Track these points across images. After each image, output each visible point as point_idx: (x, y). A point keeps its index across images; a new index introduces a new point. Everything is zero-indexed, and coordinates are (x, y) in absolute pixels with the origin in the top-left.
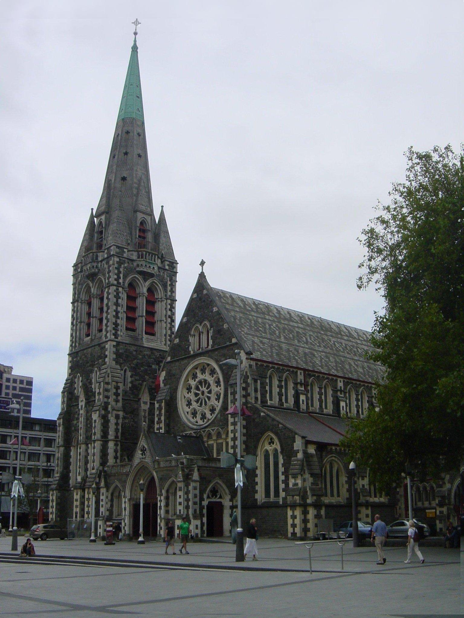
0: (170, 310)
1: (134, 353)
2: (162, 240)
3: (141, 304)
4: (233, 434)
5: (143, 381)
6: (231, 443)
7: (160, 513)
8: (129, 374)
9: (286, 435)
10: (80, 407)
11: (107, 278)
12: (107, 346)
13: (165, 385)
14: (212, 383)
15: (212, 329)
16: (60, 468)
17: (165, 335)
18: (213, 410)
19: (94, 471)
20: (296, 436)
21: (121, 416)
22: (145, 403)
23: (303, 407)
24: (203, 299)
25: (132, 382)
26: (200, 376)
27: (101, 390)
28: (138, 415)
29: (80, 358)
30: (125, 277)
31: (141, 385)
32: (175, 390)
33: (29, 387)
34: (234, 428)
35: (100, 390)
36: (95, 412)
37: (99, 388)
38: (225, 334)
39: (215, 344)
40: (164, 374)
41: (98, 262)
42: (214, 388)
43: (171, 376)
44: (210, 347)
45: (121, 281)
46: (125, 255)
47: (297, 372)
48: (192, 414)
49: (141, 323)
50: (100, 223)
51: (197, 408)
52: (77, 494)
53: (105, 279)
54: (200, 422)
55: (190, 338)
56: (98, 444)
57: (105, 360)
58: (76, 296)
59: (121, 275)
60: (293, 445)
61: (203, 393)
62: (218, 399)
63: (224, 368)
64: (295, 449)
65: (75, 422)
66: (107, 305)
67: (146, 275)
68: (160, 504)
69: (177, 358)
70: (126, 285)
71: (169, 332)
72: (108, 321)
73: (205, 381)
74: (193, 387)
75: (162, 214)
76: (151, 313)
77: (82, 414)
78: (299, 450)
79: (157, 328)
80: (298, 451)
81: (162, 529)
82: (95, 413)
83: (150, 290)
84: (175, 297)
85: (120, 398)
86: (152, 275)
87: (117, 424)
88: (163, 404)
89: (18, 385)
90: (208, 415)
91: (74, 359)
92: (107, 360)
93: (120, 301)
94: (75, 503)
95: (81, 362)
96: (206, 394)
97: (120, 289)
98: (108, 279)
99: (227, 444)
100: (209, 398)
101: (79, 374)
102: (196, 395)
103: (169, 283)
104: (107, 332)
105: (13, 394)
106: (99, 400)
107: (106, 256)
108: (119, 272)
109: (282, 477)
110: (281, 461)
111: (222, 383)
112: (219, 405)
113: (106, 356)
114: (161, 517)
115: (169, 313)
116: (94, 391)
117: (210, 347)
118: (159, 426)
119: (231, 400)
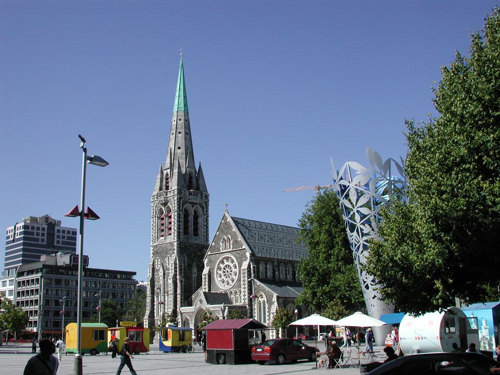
0: (206, 222)
1: (189, 247)
2: (200, 182)
3: (191, 218)
5: (194, 261)
6: (243, 297)
8: (186, 258)
10: (160, 276)
13: (207, 266)
14: (232, 267)
17: (204, 236)
18: (233, 281)
21: (184, 281)
22: (195, 273)
23: (277, 278)
25: (188, 263)
26: (226, 263)
27: (173, 267)
28: (191, 280)
30: (183, 207)
31: (193, 264)
32: (213, 269)
33: (74, 236)
37: (172, 267)
40: (206, 260)
41: (168, 197)
42: (234, 270)
44: (231, 249)
45: (181, 208)
46: (183, 194)
47: (274, 261)
49: (191, 229)
50: (167, 174)
51: (225, 279)
54: (226, 286)
59: (181, 205)
61: (228, 272)
62: (236, 275)
66: (174, 221)
67: (193, 204)
70: (183, 210)
71: (206, 234)
72: (175, 231)
73: (229, 265)
74: (223, 268)
75: (200, 166)
76: (196, 223)
79: (199, 232)
80: (274, 302)
83: (195, 212)
84: (208, 214)
85: (183, 271)
86: (196, 204)
87: (181, 285)
88: (207, 276)
89: (66, 235)
90: (231, 282)
93: (181, 219)
96: (229, 270)
97: (181, 213)
98: (174, 207)
99: (241, 297)
100: (231, 274)
102: (224, 272)
103: (205, 207)
104: (175, 236)
105: (62, 242)
106: (172, 273)
107: (172, 194)
108: (180, 204)
109: (267, 314)
110: (267, 306)
111: (237, 267)
112: (236, 278)
113: (175, 249)
115: (206, 223)
117: (231, 249)
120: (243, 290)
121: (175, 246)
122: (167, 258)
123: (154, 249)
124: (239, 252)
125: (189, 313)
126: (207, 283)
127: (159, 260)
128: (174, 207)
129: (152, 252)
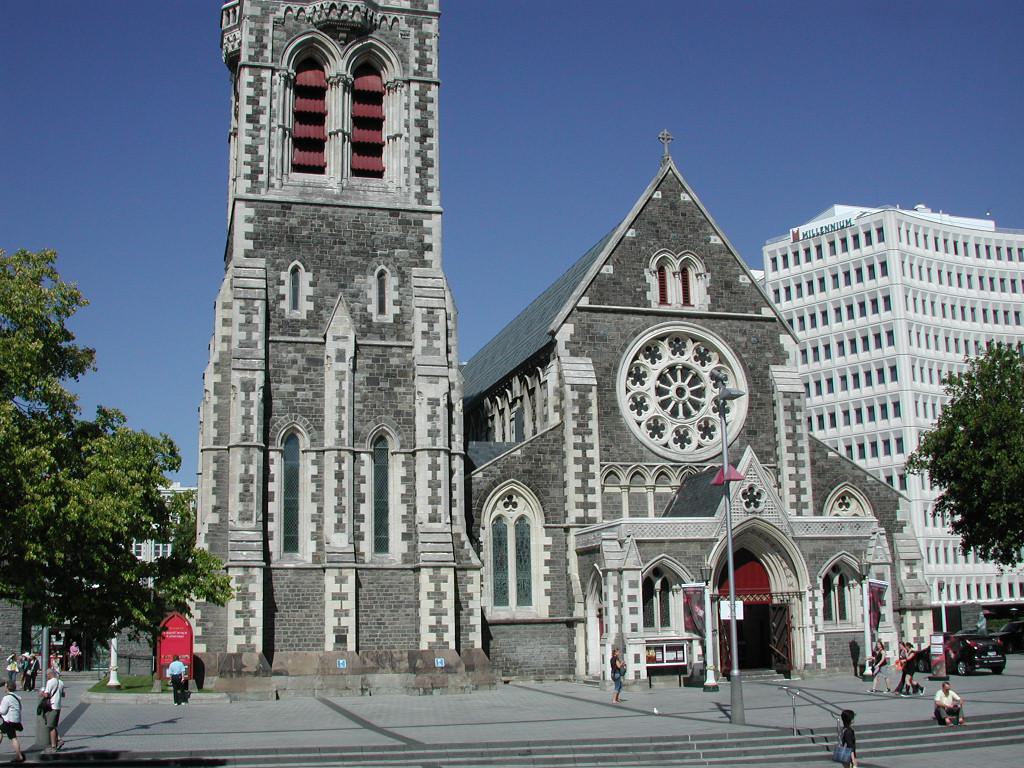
4: (794, 482)
7: (814, 622)
9: (881, 495)
11: (412, 60)
12: (426, 223)
15: (709, 275)
16: (257, 508)
18: (707, 430)
19: (436, 526)
20: (900, 499)
24: (681, 210)
27: (439, 328)
29: (303, 223)
34: (797, 472)
35: (431, 325)
36: (435, 379)
38: (743, 293)
39: (719, 307)
43: (591, 338)
48: (649, 427)
52: (341, 580)
53: (403, 60)
55: (646, 273)
56: (442, 459)
57: (421, 254)
58: (268, 53)
60: (894, 513)
61: (680, 392)
63: (744, 356)
64: (898, 519)
65: (287, 387)
66: (421, 123)
68: (814, 606)
69: (609, 305)
72: (427, 163)
77: (343, 373)
78: (905, 522)
81: (820, 654)
82: (431, 382)
88: (593, 396)
91: (270, 219)
92: (428, 256)
94: (331, 605)
95: (305, 233)
98: (423, 62)
101: (296, 262)
104: (426, 190)
113: (429, 247)
114: (816, 630)
116: (374, 320)
118: (583, 440)
119: (786, 421)
120: (792, 470)
121: (429, 232)
122: (373, 280)
123: (262, 215)
124: (747, 325)
125: (679, 547)
126: (594, 425)
127: (305, 277)
128: (423, 62)
129: (250, 228)
